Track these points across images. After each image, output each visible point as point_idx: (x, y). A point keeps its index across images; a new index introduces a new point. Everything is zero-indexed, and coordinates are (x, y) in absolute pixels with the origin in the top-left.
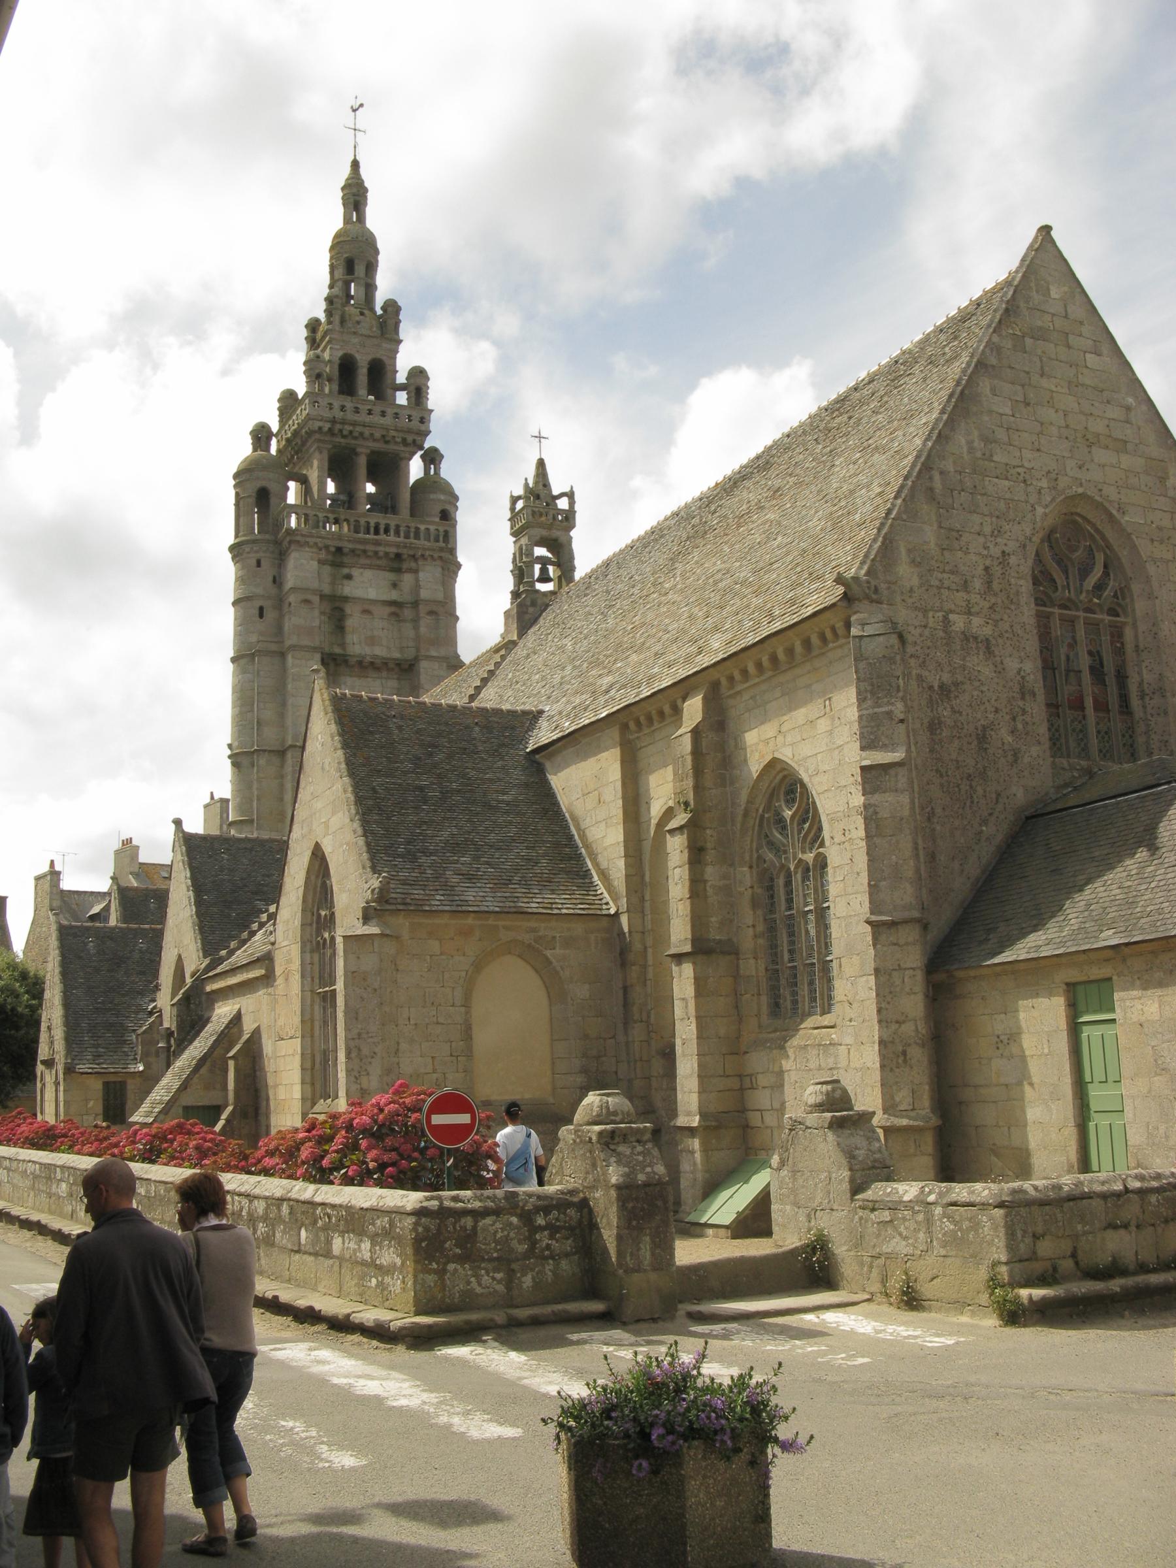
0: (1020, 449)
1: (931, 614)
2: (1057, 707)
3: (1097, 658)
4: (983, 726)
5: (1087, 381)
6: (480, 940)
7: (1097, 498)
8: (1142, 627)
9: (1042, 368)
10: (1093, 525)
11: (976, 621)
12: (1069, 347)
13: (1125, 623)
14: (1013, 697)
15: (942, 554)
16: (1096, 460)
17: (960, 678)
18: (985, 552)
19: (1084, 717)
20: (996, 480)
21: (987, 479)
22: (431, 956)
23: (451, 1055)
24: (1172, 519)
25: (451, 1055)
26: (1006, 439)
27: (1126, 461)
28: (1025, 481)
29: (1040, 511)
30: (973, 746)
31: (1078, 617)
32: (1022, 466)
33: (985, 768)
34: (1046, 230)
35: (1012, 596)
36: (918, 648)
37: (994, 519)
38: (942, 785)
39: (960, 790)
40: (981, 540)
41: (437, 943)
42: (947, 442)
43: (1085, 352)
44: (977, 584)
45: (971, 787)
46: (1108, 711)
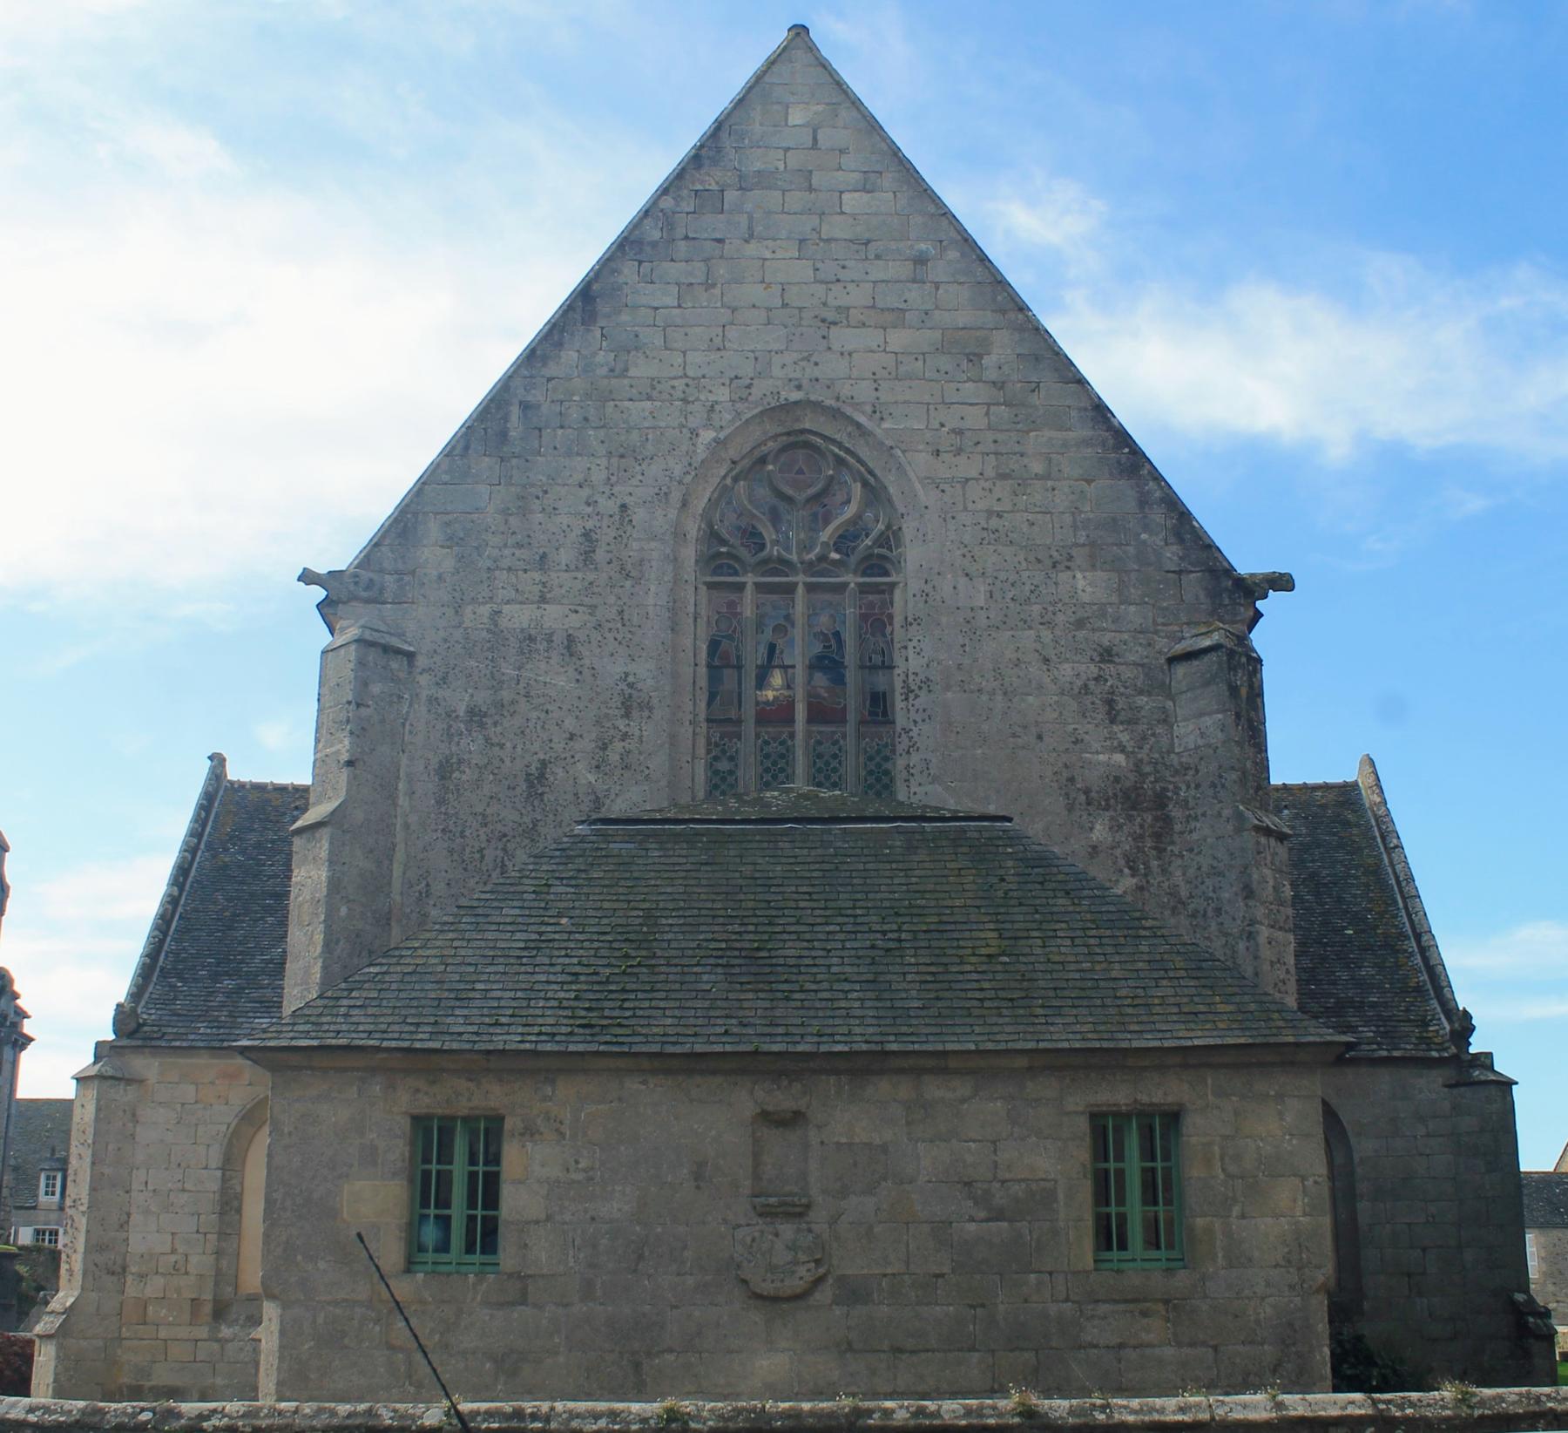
0: (684, 353)
1: (469, 609)
2: (739, 722)
3: (833, 642)
4: (544, 763)
5: (838, 234)
6: (250, 1085)
7: (830, 402)
8: (915, 586)
9: (750, 228)
10: (840, 445)
11: (551, 609)
12: (810, 189)
13: (893, 585)
14: (607, 715)
15: (506, 522)
16: (836, 346)
17: (506, 695)
18: (590, 510)
19: (792, 736)
20: (627, 404)
21: (612, 403)
22: (183, 1104)
23: (198, 1232)
24: (987, 414)
25: (198, 1232)
26: (659, 342)
27: (898, 339)
28: (685, 401)
29: (707, 436)
30: (518, 790)
31: (796, 584)
32: (686, 376)
33: (535, 823)
34: (800, 32)
35: (629, 567)
36: (437, 658)
37: (614, 460)
38: (451, 851)
39: (483, 857)
40: (586, 492)
41: (193, 1088)
42: (545, 364)
43: (841, 192)
44: (565, 556)
45: (505, 850)
46: (843, 721)
